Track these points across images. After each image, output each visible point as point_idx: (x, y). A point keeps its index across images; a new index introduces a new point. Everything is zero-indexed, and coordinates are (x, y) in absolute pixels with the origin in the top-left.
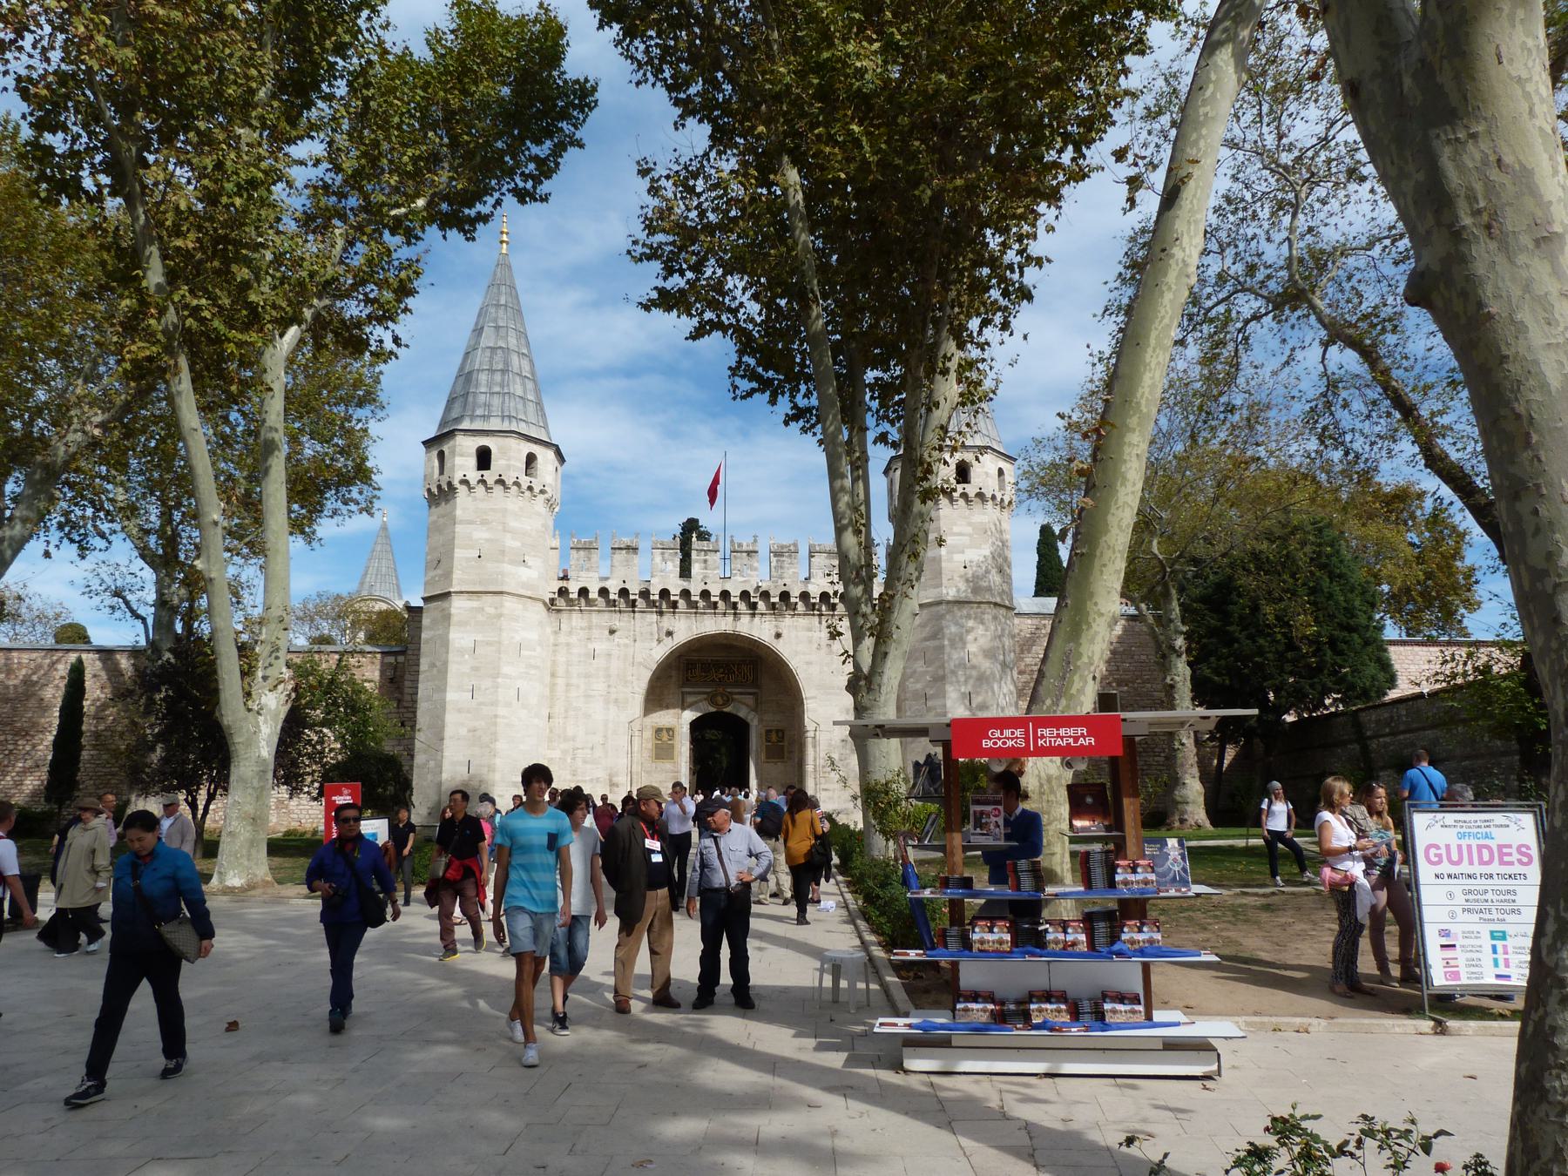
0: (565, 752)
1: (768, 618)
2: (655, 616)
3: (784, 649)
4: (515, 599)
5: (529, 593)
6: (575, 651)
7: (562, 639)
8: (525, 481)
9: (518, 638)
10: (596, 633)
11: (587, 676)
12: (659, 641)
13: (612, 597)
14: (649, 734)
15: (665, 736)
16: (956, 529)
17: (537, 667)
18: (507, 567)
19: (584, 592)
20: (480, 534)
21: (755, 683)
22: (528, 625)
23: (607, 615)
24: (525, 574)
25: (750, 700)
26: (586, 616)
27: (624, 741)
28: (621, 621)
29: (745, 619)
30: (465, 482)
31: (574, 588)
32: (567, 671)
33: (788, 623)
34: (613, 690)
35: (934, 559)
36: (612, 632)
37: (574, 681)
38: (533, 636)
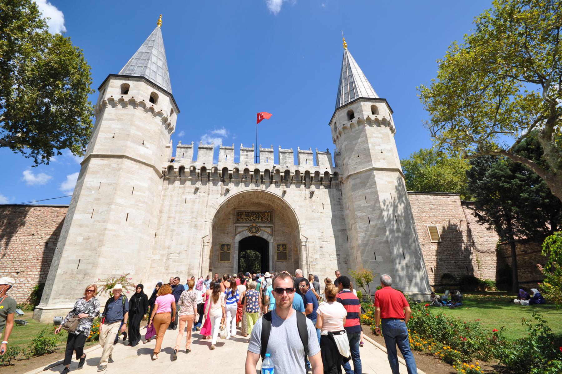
0: (162, 255)
3: (287, 199)
4: (133, 162)
6: (175, 199)
8: (149, 104)
9: (132, 184)
10: (188, 190)
11: (180, 212)
12: (221, 194)
13: (197, 171)
14: (218, 247)
16: (374, 135)
18: (129, 144)
19: (182, 169)
20: (116, 126)
21: (271, 221)
22: (146, 179)
24: (142, 150)
25: (269, 230)
27: (199, 248)
30: (111, 100)
31: (176, 166)
32: (169, 210)
35: (365, 149)
38: (145, 184)
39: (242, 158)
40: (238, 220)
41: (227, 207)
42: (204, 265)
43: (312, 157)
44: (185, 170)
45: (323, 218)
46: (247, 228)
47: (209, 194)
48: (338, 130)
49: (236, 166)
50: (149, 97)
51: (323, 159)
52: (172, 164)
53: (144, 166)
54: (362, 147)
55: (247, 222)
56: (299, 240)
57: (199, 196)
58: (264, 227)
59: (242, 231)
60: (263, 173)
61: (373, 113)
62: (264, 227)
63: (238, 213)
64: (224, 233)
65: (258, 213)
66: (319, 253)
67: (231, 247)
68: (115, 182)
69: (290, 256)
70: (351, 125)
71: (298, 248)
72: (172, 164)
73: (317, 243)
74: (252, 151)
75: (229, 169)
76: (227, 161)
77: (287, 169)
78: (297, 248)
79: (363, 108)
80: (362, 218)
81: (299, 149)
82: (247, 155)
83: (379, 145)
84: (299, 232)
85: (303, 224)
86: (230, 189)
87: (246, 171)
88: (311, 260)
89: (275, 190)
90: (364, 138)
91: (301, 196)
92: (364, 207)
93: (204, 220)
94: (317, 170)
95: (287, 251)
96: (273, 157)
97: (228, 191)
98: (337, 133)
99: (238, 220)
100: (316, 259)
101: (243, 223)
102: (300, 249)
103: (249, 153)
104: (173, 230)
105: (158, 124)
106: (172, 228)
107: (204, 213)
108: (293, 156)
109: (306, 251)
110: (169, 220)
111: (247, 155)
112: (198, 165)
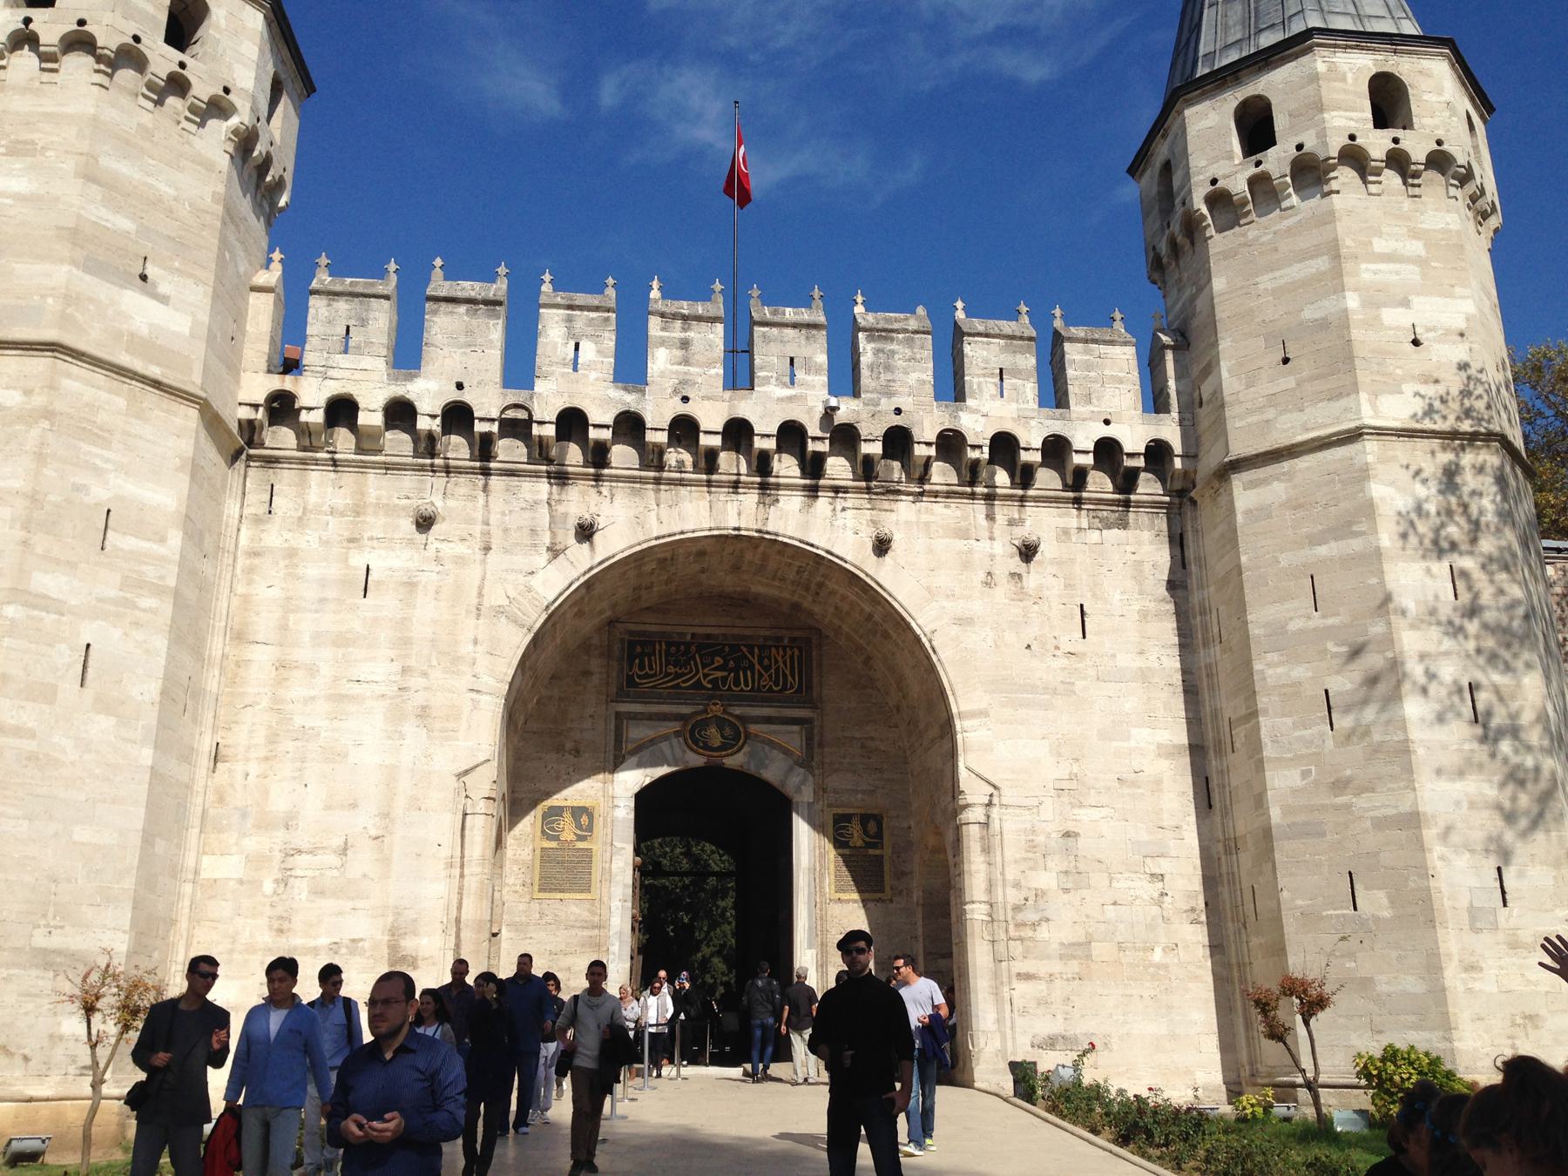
0: (257, 861)
1: (851, 500)
2: (543, 488)
3: (898, 581)
4: (99, 377)
5: (154, 371)
7: (273, 537)
9: (100, 493)
10: (375, 524)
11: (342, 641)
12: (555, 552)
15: (568, 834)
16: (1380, 245)
17: (158, 591)
21: (805, 694)
23: (408, 481)
26: (348, 478)
28: (454, 498)
29: (791, 503)
31: (312, 394)
32: (284, 627)
33: (903, 516)
34: (415, 682)
35: (1323, 325)
36: (425, 523)
37: (303, 654)
39: (660, 361)
40: (631, 682)
41: (580, 614)
42: (466, 915)
43: (1029, 361)
44: (363, 419)
45: (1079, 684)
46: (677, 726)
47: (487, 549)
48: (1179, 210)
49: (629, 401)
50: (163, 18)
51: (1088, 367)
52: (287, 383)
53: (153, 395)
54: (1309, 314)
55: (677, 696)
56: (955, 791)
57: (437, 559)
58: (768, 720)
59: (652, 742)
60: (770, 444)
61: (1381, 121)
62: (768, 720)
63: (632, 644)
64: (559, 749)
65: (735, 648)
66: (1056, 863)
67: (599, 823)
68: (17, 484)
69: (901, 875)
70: (1253, 182)
71: (950, 836)
72: (287, 383)
73: (1048, 811)
74: (713, 320)
75: (595, 416)
76: (576, 369)
77: (897, 421)
78: (939, 833)
79: (1330, 92)
80: (1292, 691)
81: (960, 315)
82: (685, 344)
83: (1405, 303)
84: (952, 755)
85: (973, 715)
86: (601, 522)
87: (684, 429)
88: (1013, 896)
89: (832, 527)
90: (1322, 263)
91: (966, 565)
92: (1301, 631)
93: (466, 681)
94: (1057, 427)
95: (887, 851)
96: (822, 358)
97: (586, 532)
98: (1176, 227)
99: (631, 682)
100: (1040, 894)
101: (661, 700)
102: (958, 840)
103: (697, 333)
104: (304, 734)
105: (209, 166)
106: (298, 721)
107: (466, 649)
108: (927, 354)
109: (987, 850)
110: (280, 682)
111: (685, 344)
112: (427, 397)
